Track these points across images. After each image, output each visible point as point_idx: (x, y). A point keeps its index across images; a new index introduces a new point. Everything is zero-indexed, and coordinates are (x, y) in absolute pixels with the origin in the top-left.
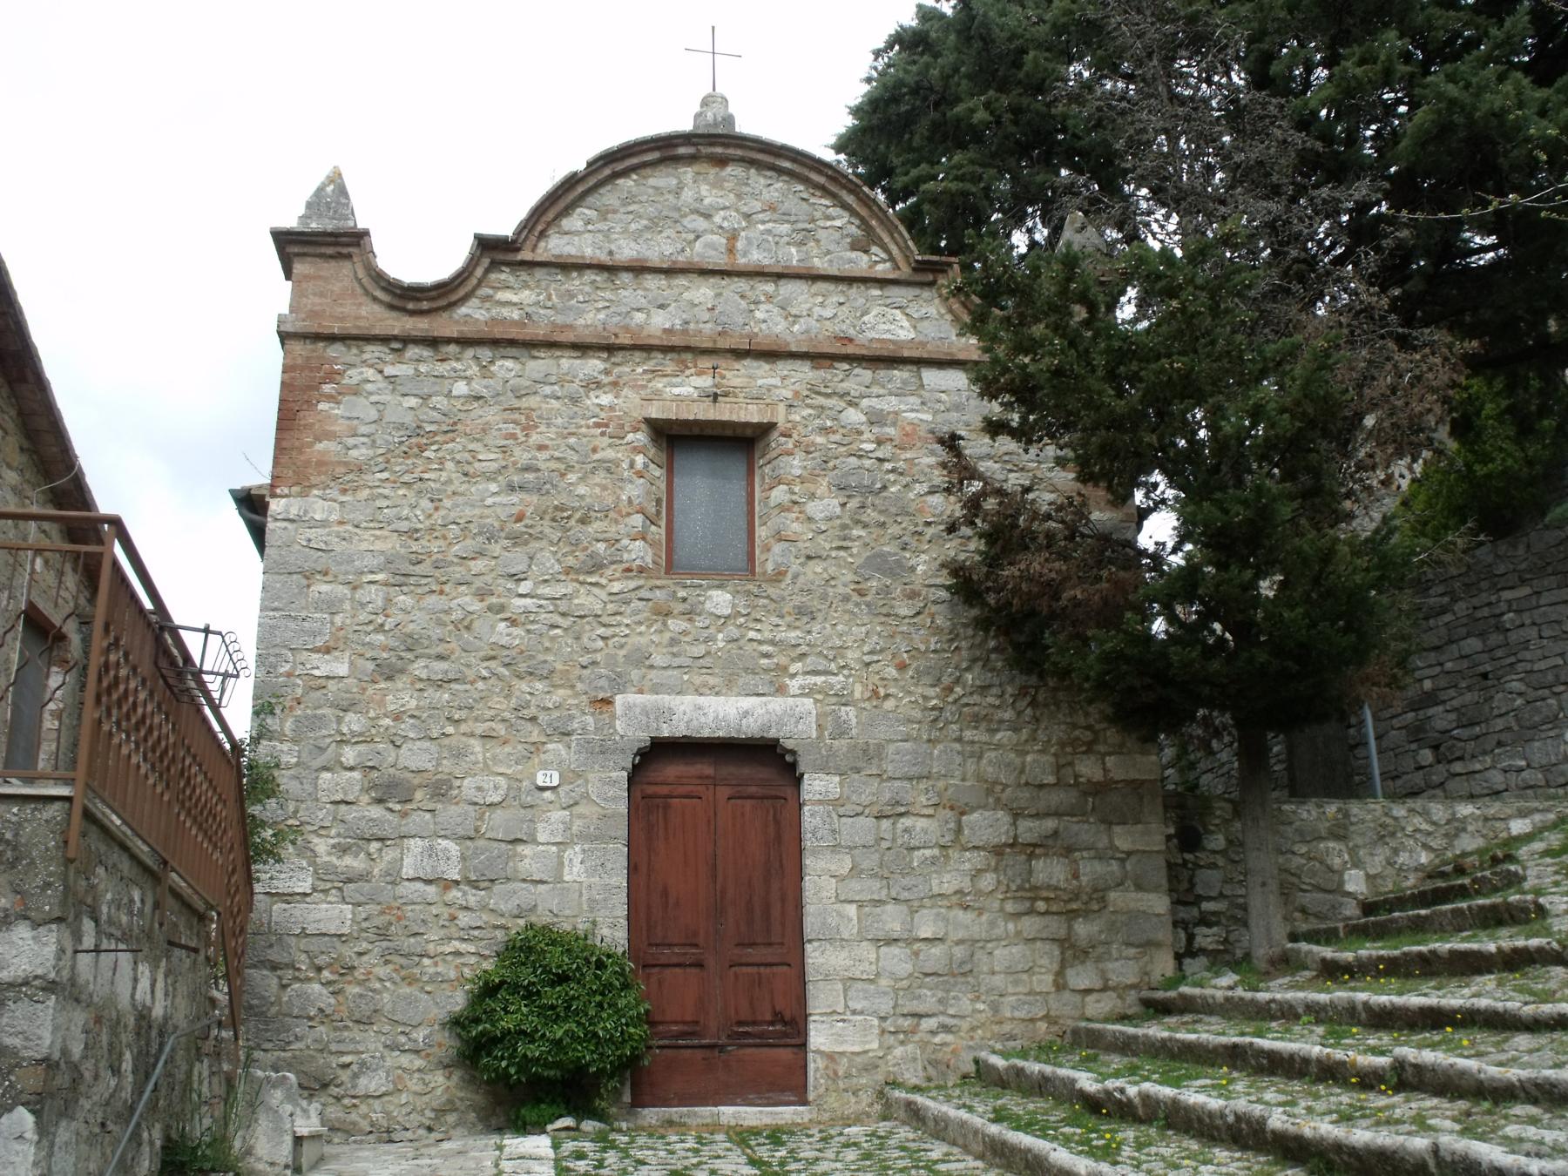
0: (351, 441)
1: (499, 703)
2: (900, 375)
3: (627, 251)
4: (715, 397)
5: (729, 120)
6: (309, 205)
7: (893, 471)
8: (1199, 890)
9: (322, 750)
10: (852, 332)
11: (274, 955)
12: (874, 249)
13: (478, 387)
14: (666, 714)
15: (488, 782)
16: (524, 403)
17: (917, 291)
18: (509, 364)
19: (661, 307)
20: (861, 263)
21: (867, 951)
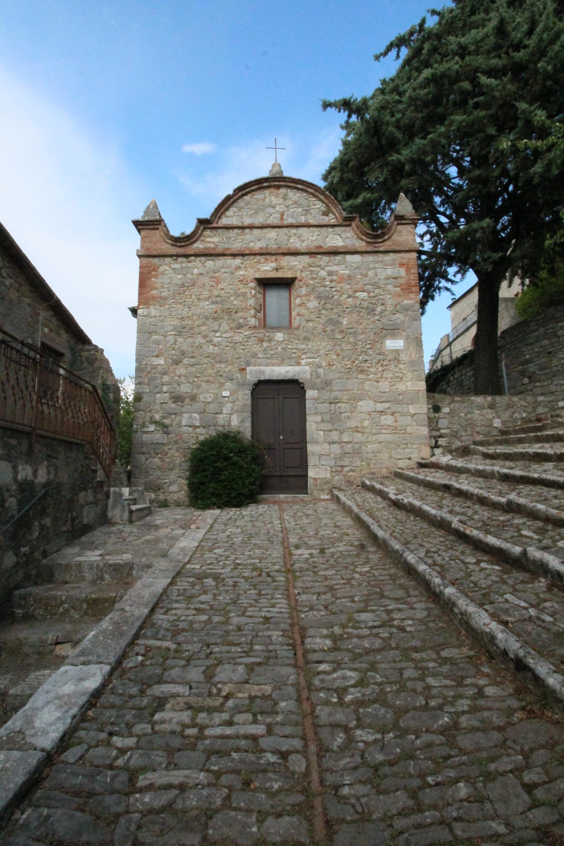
0: (162, 290)
1: (210, 371)
2: (338, 258)
3: (247, 221)
4: (277, 269)
5: (281, 172)
6: (145, 212)
7: (336, 291)
8: (440, 426)
9: (156, 387)
10: (322, 245)
11: (144, 450)
12: (330, 215)
13: (201, 271)
14: (262, 372)
15: (207, 395)
16: (217, 275)
17: (343, 228)
18: (211, 262)
19: (259, 240)
20: (326, 220)
21: (326, 446)
